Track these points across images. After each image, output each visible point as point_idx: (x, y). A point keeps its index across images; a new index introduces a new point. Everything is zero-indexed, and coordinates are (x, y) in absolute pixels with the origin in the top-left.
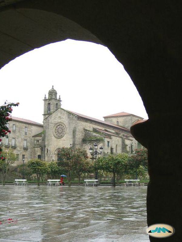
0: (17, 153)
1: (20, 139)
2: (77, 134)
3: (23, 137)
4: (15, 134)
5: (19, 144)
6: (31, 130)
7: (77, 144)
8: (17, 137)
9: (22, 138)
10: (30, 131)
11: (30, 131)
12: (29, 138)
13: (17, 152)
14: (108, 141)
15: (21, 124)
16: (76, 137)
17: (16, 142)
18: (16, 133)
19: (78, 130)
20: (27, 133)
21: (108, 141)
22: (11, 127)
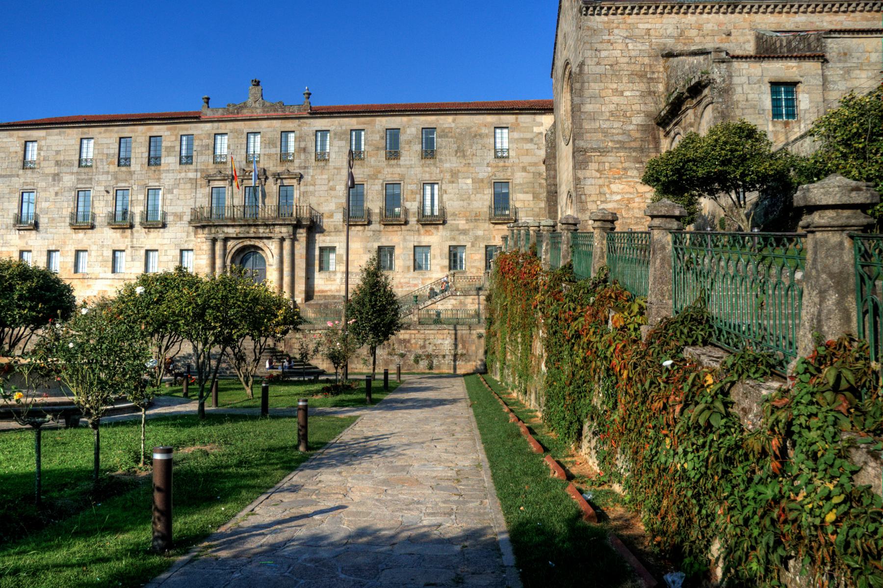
0: (454, 243)
1: (469, 181)
2: (587, 93)
3: (484, 172)
4: (435, 164)
5: (465, 204)
6: (529, 136)
7: (594, 150)
8: (448, 176)
9: (481, 176)
10: (531, 140)
11: (531, 140)
12: (524, 169)
13: (454, 239)
14: (775, 85)
15: (465, 120)
16: (588, 108)
17: (445, 197)
18: (441, 160)
19: (600, 69)
20: (512, 153)
21: (775, 85)
22: (409, 142)
